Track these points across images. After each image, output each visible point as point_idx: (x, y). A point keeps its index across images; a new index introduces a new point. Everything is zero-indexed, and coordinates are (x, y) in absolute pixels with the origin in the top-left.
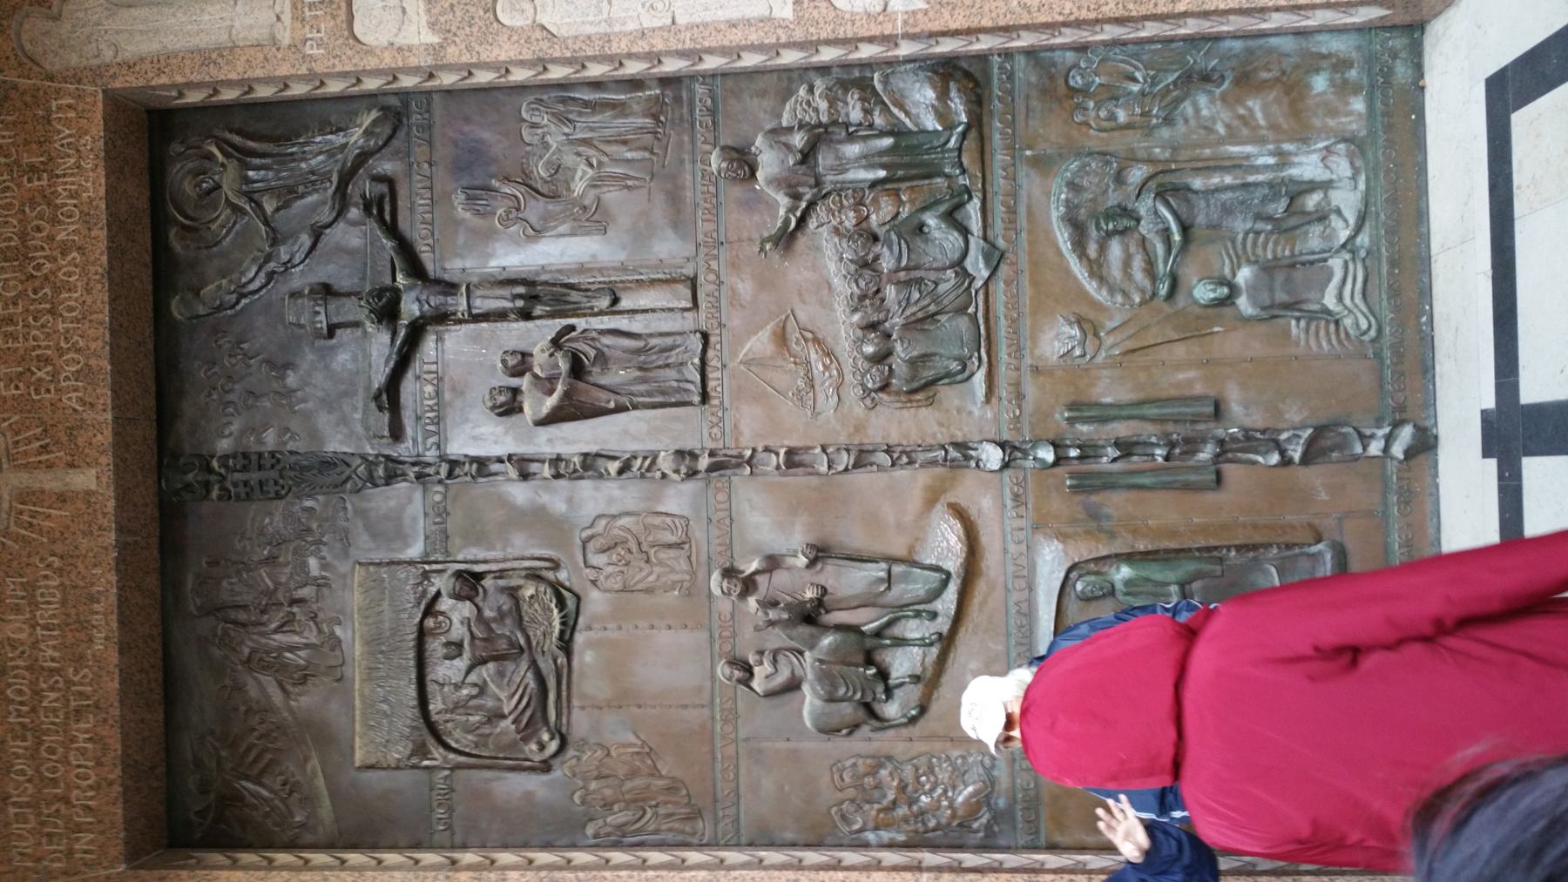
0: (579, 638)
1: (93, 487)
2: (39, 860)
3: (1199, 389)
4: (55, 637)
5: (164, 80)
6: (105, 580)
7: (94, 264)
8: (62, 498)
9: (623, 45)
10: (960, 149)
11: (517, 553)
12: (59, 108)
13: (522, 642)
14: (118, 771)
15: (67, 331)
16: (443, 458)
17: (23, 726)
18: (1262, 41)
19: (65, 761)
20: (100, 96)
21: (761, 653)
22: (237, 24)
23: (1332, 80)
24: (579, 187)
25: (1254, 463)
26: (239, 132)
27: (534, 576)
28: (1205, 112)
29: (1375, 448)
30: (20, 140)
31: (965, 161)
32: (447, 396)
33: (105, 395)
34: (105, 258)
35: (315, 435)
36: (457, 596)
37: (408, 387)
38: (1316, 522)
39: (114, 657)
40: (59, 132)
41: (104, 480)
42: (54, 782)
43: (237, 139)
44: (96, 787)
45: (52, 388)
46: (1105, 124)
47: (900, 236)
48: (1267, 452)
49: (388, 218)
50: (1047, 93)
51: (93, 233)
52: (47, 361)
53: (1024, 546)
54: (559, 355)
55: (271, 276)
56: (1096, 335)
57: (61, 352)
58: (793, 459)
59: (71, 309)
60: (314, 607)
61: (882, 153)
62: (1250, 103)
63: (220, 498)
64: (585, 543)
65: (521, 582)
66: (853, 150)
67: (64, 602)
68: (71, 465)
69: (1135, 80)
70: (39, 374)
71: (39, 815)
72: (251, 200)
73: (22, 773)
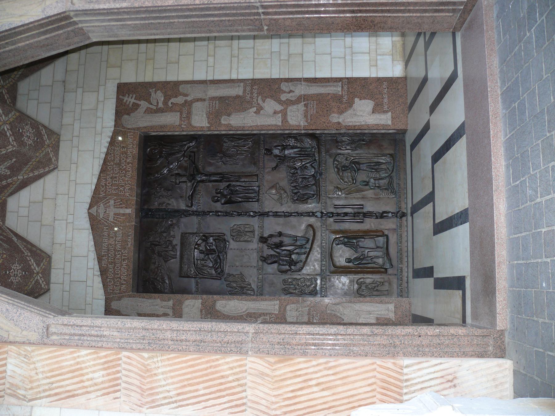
2: (114, 290)
8: (124, 215)
14: (132, 272)
17: (112, 262)
19: (120, 270)
38: (383, 230)
41: (133, 211)
42: (118, 274)
44: (127, 275)
47: (301, 168)
52: (123, 186)
57: (126, 184)
59: (129, 176)
61: (298, 152)
67: (122, 236)
68: (126, 208)
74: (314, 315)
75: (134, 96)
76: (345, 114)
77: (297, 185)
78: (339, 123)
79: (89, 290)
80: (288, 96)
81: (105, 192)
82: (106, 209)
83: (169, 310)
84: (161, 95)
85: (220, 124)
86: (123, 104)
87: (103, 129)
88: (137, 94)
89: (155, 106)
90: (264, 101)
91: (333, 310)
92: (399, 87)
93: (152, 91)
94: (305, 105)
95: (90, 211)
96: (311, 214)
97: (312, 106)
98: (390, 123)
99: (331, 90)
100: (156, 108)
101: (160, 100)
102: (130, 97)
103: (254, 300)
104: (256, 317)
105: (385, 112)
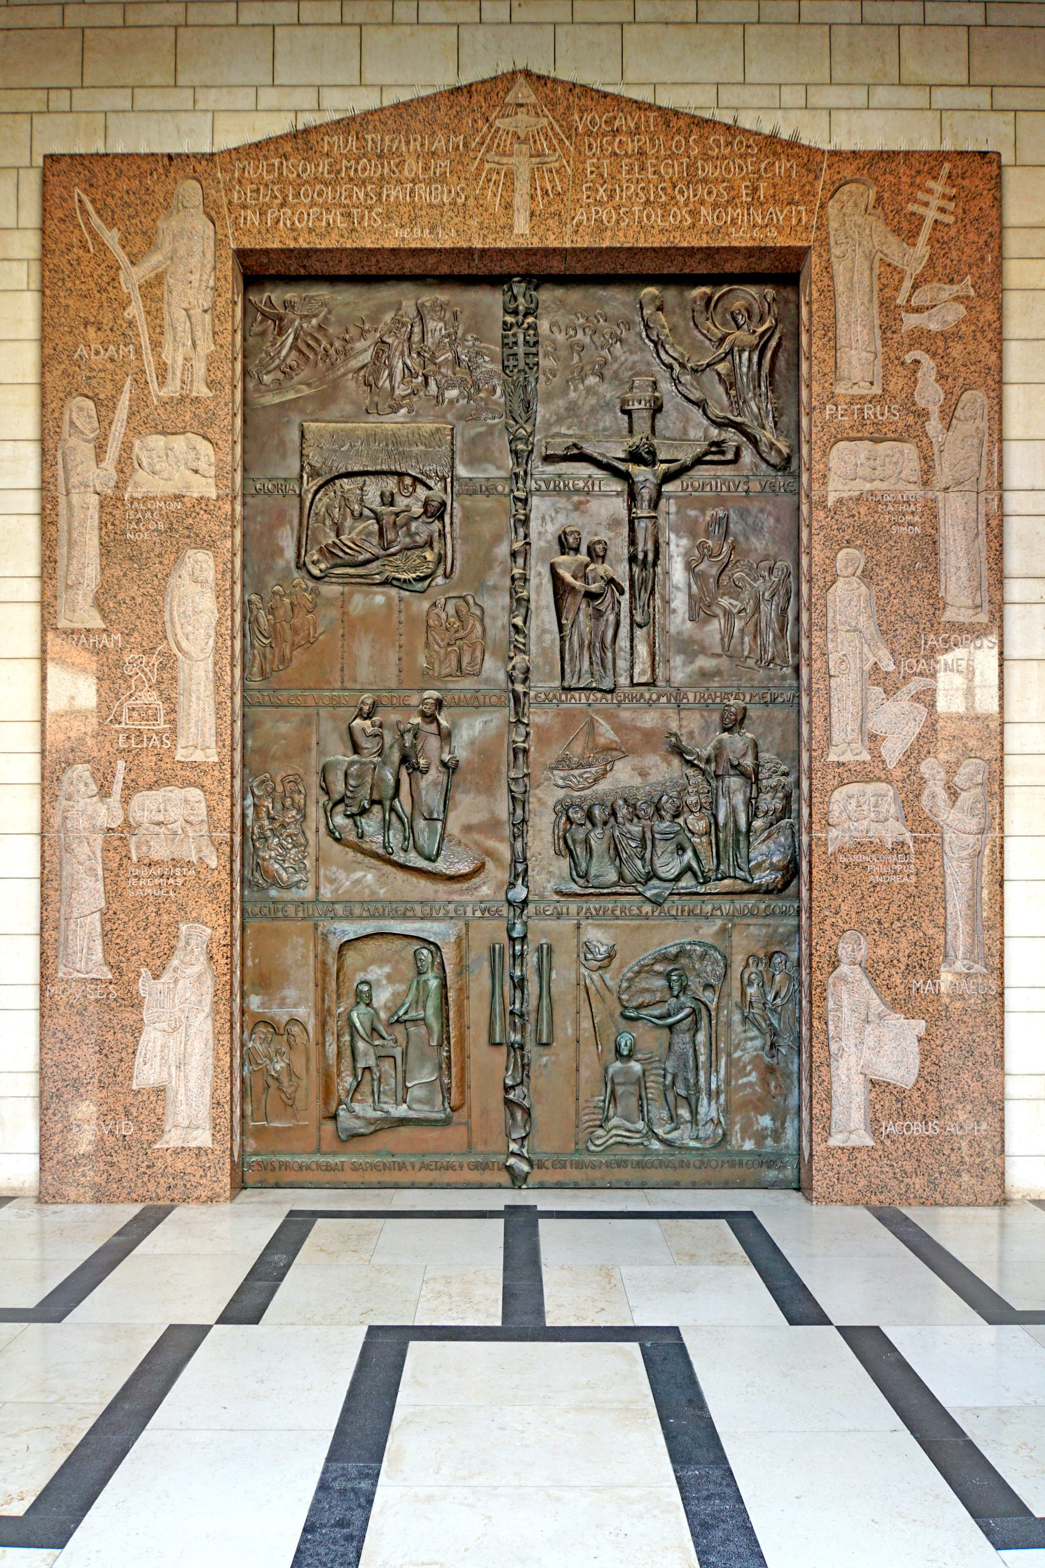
0: (393, 592)
1: (516, 231)
2: (240, 182)
3: (558, 1033)
4: (404, 198)
5: (815, 295)
6: (446, 240)
7: (682, 236)
8: (508, 206)
9: (818, 640)
10: (735, 877)
11: (457, 547)
12: (799, 212)
13: (392, 550)
14: (305, 246)
15: (633, 214)
16: (529, 493)
17: (339, 172)
18: (796, 1084)
20: (806, 244)
21: (381, 726)
22: (853, 352)
23: (766, 1128)
24: (725, 601)
25: (507, 1069)
26: (779, 345)
27: (441, 559)
28: (749, 1044)
29: (514, 1147)
30: (777, 180)
31: (726, 881)
32: (576, 498)
33: (585, 242)
34: (685, 244)
35: (549, 397)
36: (426, 504)
37: (584, 470)
38: (465, 1108)
39: (389, 244)
40: (781, 211)
41: (521, 240)
42: (297, 195)
43: (773, 343)
44: (293, 229)
45: (591, 200)
46: (746, 976)
47: (677, 833)
48: (514, 1078)
49: (708, 458)
50: (770, 939)
51: (704, 236)
52: (611, 197)
53: (452, 914)
54: (602, 583)
55: (670, 367)
56: (600, 968)
57: (617, 208)
58: (519, 753)
59: (648, 217)
60: (422, 393)
62: (754, 1074)
63: (505, 323)
64: (463, 598)
65: (436, 550)
66: (739, 799)
67: (431, 206)
68: (532, 214)
69: (775, 998)
70: (601, 190)
71: (273, 183)
72: (727, 354)
73: (305, 170)
74: (171, 881)
75: (949, 219)
76: (865, 983)
77: (620, 820)
78: (835, 964)
79: (244, 99)
80: (936, 788)
81: (590, 134)
82: (526, 141)
83: (178, 383)
84: (949, 318)
85: (835, 544)
86: (918, 180)
87: (824, 114)
88: (953, 232)
89: (908, 301)
90: (916, 698)
91: (188, 943)
92: (965, 1177)
93: (966, 286)
94: (903, 843)
95: (521, 79)
96: (520, 868)
97: (898, 867)
98: (835, 1141)
99: (955, 936)
100: (896, 307)
101: (930, 315)
102: (942, 203)
103: (218, 678)
104: (163, 687)
105: (874, 1125)
